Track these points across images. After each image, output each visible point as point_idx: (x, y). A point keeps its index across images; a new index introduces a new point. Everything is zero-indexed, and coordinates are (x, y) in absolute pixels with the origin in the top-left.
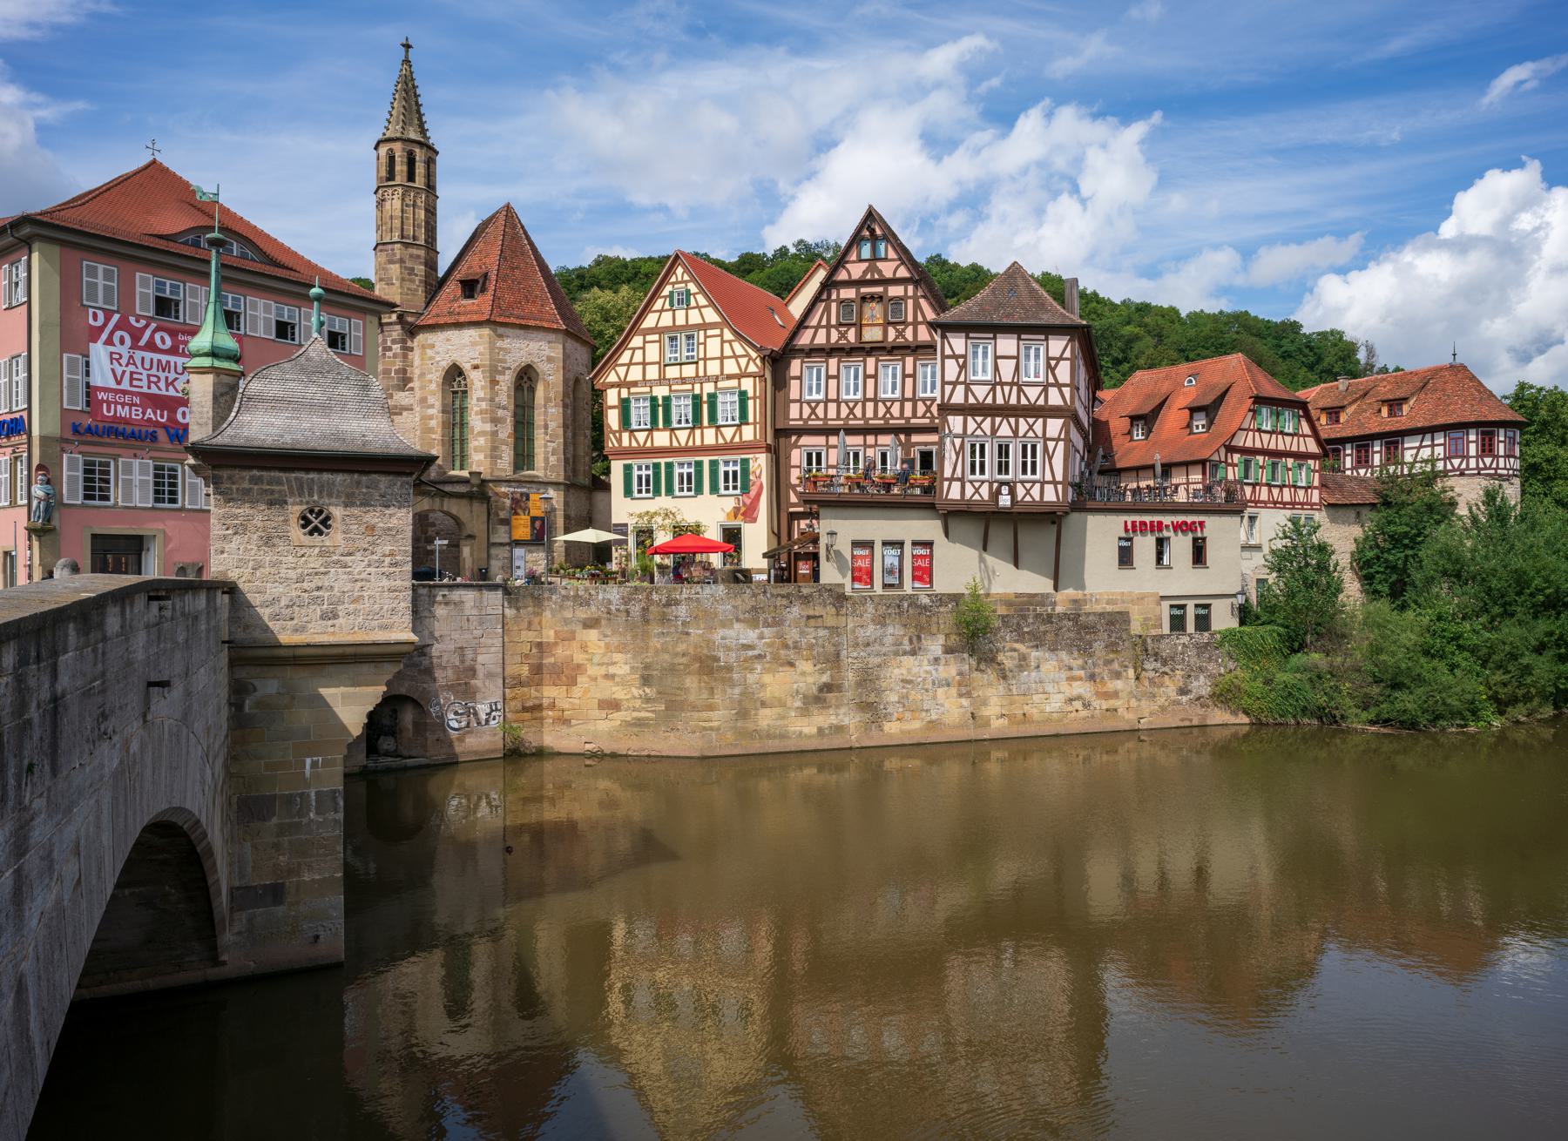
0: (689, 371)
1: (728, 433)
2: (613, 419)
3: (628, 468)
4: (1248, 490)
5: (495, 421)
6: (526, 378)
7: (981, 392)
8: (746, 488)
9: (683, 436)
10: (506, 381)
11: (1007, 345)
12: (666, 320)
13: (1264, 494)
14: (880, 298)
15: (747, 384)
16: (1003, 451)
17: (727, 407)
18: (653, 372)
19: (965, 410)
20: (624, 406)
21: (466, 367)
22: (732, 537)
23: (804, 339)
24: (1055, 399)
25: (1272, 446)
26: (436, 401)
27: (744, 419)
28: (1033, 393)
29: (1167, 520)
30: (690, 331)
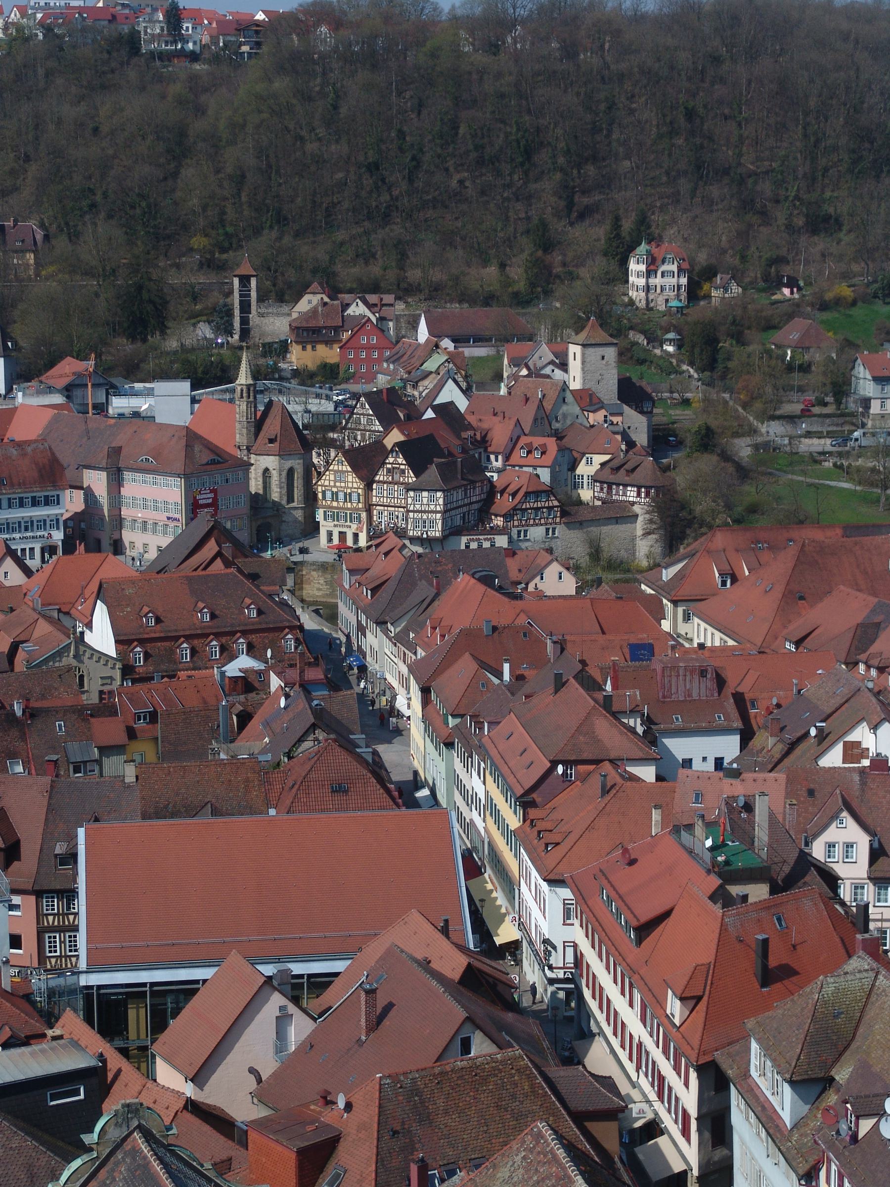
0: (343, 485)
1: (355, 505)
2: (320, 496)
3: (325, 512)
4: (524, 522)
5: (281, 488)
6: (291, 472)
7: (418, 507)
8: (360, 522)
9: (341, 504)
10: (284, 474)
11: (425, 494)
12: (336, 468)
13: (532, 522)
14: (399, 468)
15: (360, 491)
16: (424, 522)
17: (354, 497)
18: (332, 484)
19: (414, 511)
20: (324, 493)
21: (271, 469)
22: (356, 536)
23: (377, 478)
24: (438, 509)
25: (535, 506)
26: (261, 479)
27: (359, 502)
28: (432, 507)
29: (481, 537)
30: (342, 472)
